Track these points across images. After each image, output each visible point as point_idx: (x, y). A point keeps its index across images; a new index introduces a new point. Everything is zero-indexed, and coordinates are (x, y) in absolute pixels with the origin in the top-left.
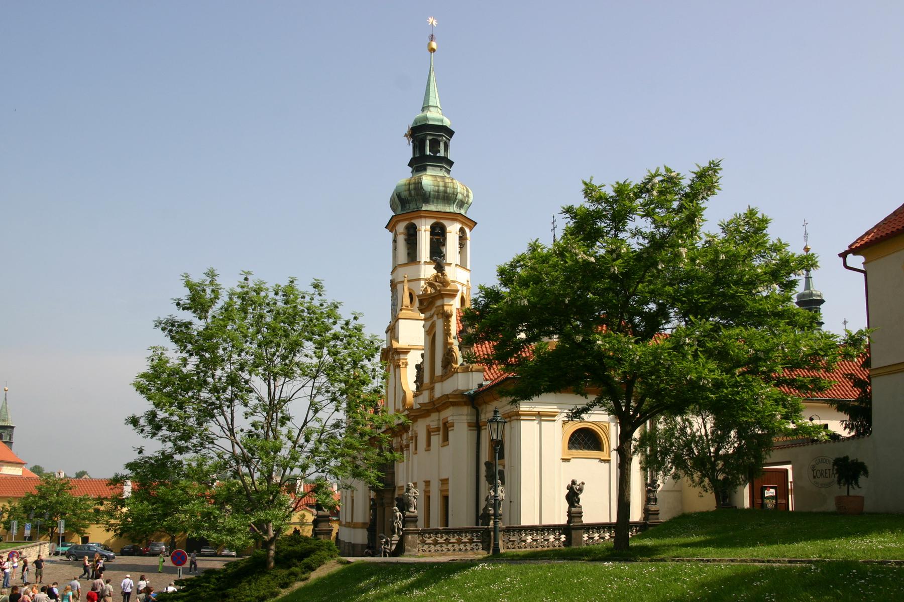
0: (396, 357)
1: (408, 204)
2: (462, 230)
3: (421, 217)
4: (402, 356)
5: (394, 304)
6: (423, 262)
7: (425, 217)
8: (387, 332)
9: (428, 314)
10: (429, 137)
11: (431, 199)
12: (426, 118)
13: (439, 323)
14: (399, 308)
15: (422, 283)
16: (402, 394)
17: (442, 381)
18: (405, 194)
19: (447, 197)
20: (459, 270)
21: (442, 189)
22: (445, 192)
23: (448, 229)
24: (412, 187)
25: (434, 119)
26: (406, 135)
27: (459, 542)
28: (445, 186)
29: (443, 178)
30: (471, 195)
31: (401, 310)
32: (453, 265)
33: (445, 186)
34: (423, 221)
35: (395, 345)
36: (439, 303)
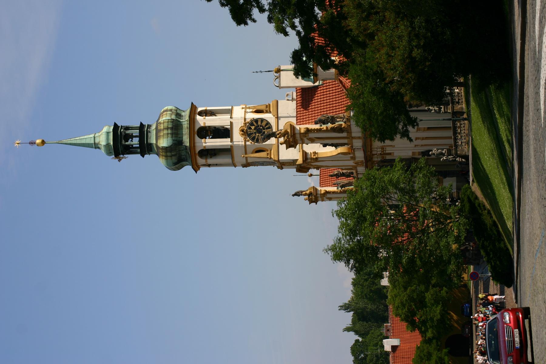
0: (309, 160)
1: (180, 156)
2: (201, 114)
3: (194, 146)
4: (309, 156)
5: (263, 164)
6: (230, 144)
7: (194, 143)
8: (282, 168)
9: (300, 142)
10: (123, 142)
11: (178, 139)
12: (108, 145)
13: (311, 135)
14: (268, 160)
15: (248, 143)
16: (341, 155)
17: (351, 133)
18: (174, 159)
19: (175, 127)
20: (234, 115)
21: (169, 131)
22: (172, 129)
23: (202, 125)
24: (169, 154)
25: (108, 139)
26: (119, 160)
27: (460, 127)
28: (167, 128)
29: (158, 131)
30: (170, 107)
31: (271, 158)
32: (232, 120)
33: (167, 128)
34: (197, 145)
35: (300, 161)
36: (298, 136)
